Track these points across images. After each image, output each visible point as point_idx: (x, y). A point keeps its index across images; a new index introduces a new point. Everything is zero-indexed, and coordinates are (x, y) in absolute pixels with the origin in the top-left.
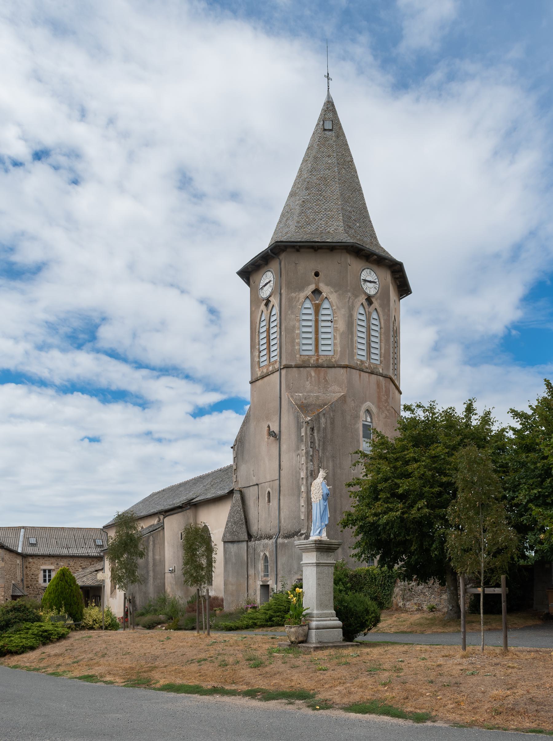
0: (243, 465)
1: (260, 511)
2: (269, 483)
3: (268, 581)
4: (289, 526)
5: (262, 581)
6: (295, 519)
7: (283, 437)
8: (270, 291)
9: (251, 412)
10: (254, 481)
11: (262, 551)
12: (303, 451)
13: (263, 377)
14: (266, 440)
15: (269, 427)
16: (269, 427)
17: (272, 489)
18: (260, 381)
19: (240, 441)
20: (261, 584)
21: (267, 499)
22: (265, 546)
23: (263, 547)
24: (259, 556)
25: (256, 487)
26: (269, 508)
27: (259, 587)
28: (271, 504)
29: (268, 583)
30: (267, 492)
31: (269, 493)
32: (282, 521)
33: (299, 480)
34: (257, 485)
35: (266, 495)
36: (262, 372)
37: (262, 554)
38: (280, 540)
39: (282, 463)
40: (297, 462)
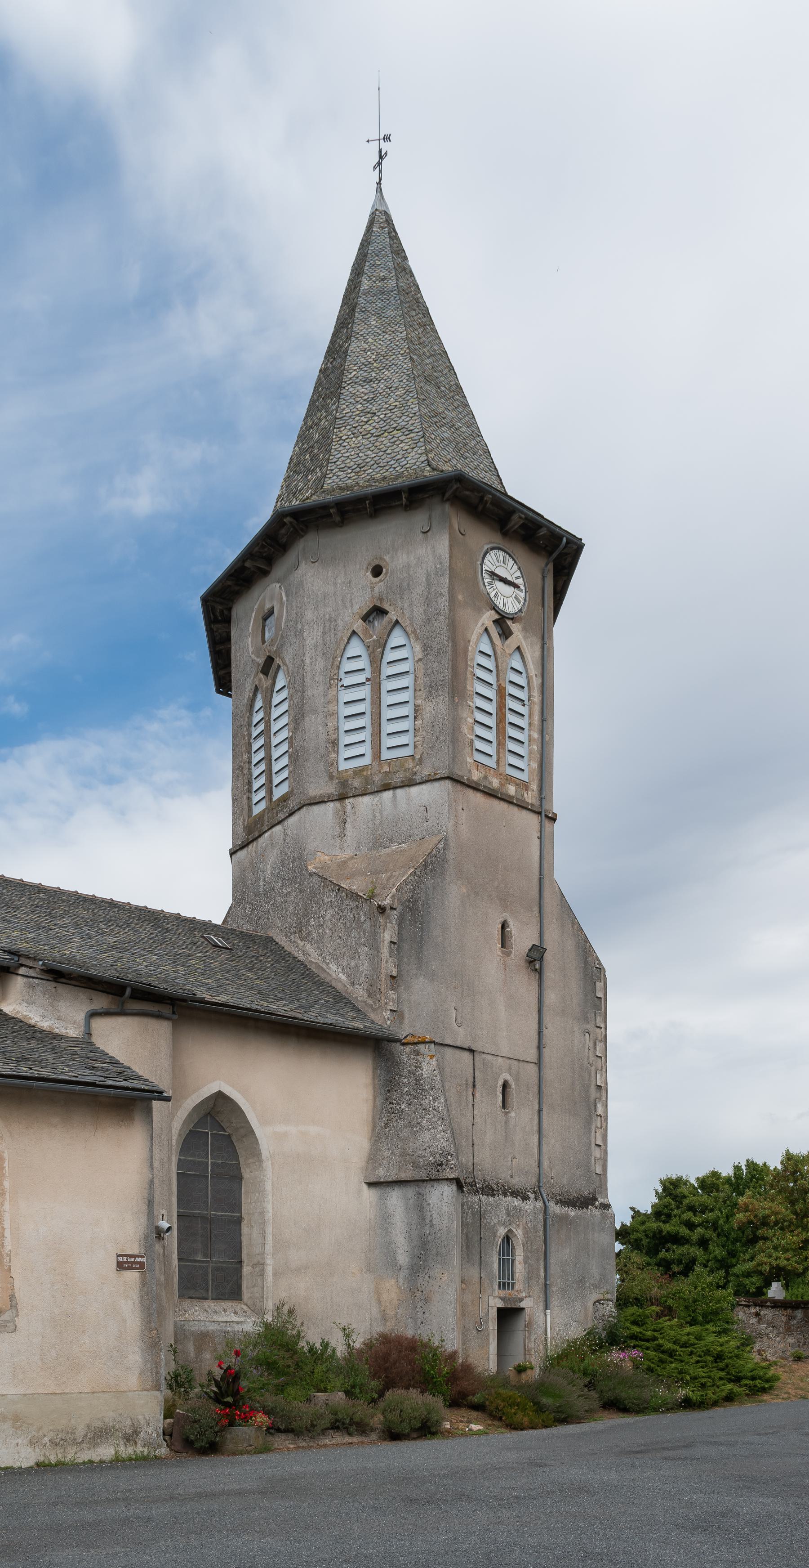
0: (422, 979)
1: (478, 1120)
2: (508, 1061)
3: (521, 1300)
4: (564, 1181)
5: (503, 1299)
6: (578, 1166)
7: (551, 974)
8: (516, 610)
9: (450, 855)
10: (461, 1037)
11: (504, 1224)
12: (598, 1030)
13: (491, 794)
14: (499, 953)
15: (504, 926)
16: (504, 926)
17: (517, 1077)
18: (479, 795)
19: (411, 909)
20: (501, 1304)
21: (500, 1098)
22: (513, 1214)
23: (508, 1214)
24: (495, 1235)
25: (466, 1055)
26: (506, 1122)
27: (493, 1313)
28: (513, 1114)
29: (522, 1305)
30: (500, 1083)
31: (505, 1086)
32: (545, 1163)
33: (589, 1086)
34: (471, 1051)
35: (500, 1089)
36: (485, 778)
37: (502, 1231)
38: (555, 1209)
39: (545, 1031)
40: (584, 1046)
